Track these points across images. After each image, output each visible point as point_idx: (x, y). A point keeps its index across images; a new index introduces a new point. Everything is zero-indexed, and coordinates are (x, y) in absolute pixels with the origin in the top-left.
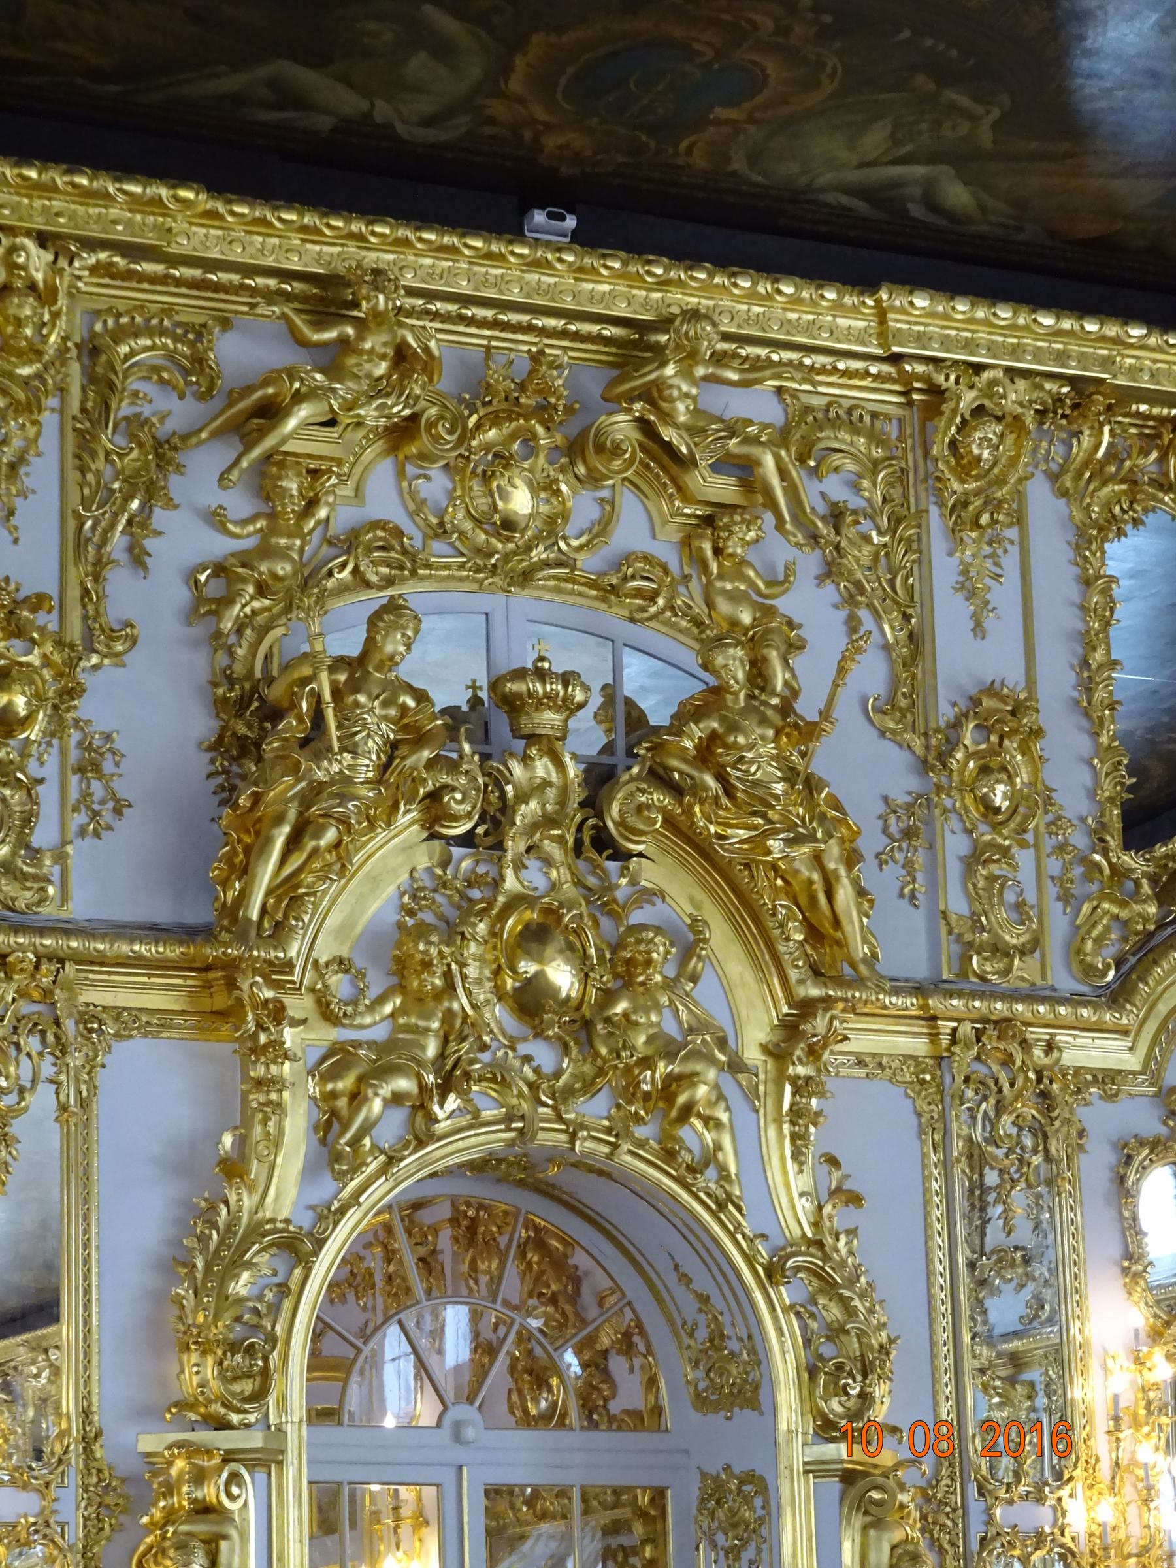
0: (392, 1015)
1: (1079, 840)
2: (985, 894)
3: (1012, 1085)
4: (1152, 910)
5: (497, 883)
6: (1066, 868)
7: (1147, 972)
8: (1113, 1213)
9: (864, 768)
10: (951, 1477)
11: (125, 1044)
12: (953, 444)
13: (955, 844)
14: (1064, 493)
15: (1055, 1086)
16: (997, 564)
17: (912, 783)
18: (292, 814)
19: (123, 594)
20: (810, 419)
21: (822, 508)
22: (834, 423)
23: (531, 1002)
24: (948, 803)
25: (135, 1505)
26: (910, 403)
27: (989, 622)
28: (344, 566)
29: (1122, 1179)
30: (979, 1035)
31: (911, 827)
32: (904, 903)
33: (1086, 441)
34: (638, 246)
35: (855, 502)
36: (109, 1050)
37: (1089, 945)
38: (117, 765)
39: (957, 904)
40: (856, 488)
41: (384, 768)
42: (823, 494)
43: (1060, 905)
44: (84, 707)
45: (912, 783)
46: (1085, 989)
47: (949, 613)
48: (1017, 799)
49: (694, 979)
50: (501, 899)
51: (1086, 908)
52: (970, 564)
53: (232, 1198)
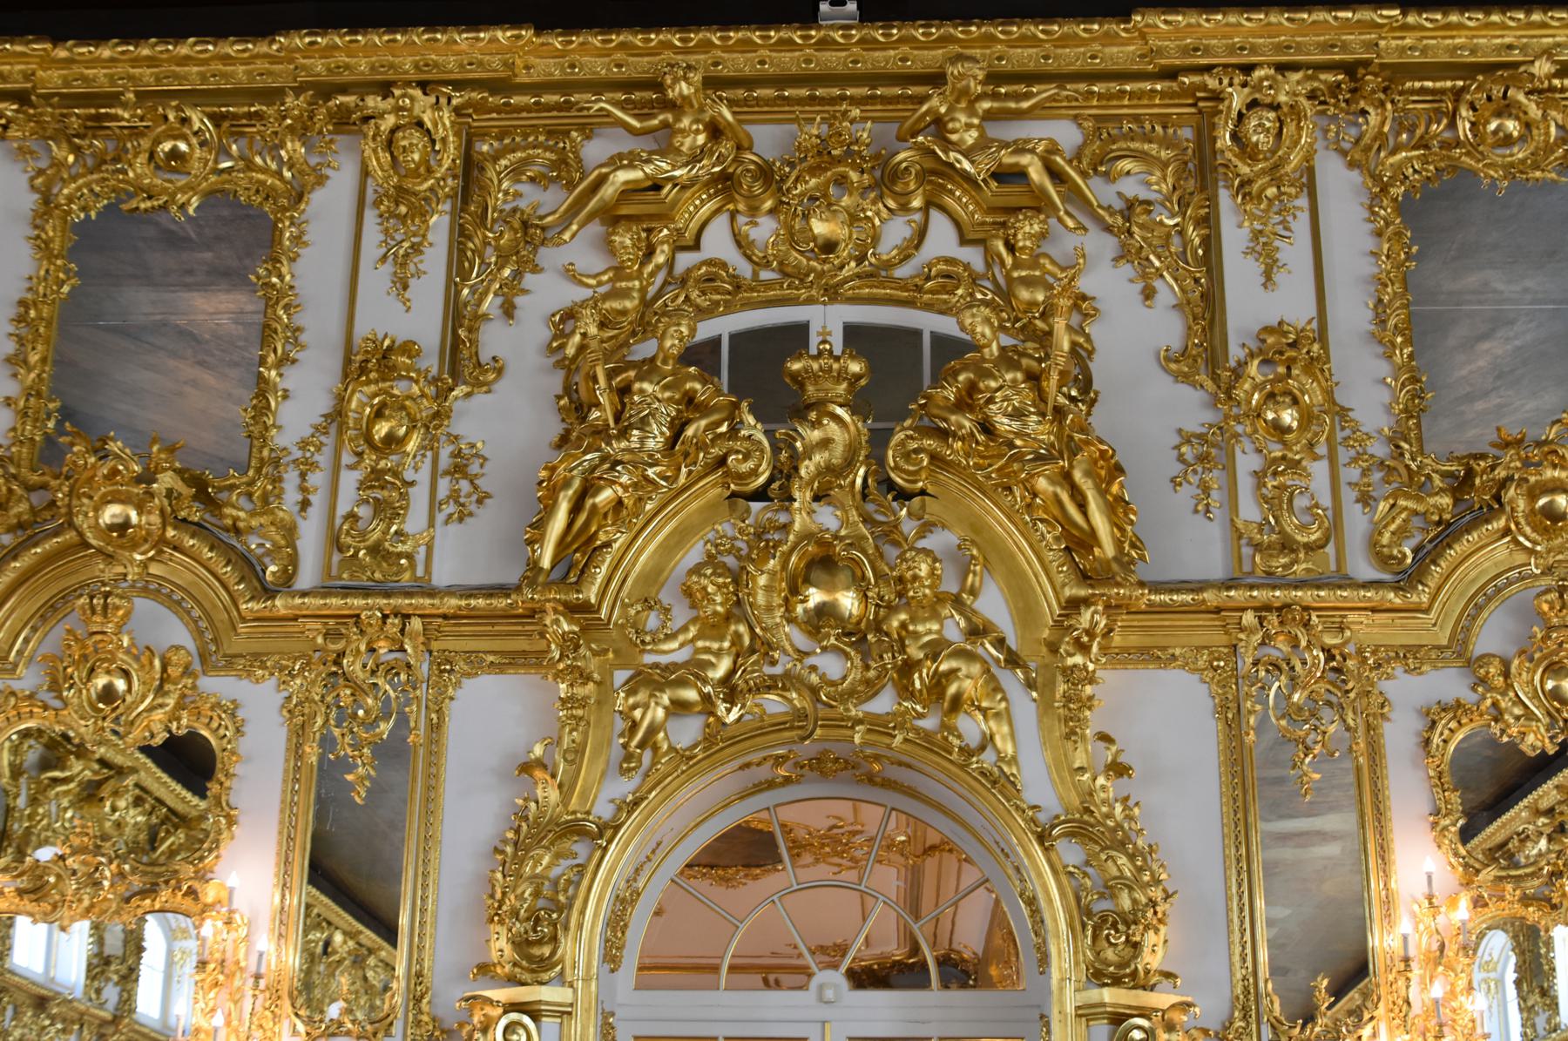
0: (692, 641)
1: (1379, 450)
2: (1277, 502)
3: (1304, 663)
4: (1446, 501)
5: (786, 528)
6: (1365, 473)
7: (1441, 555)
8: (1422, 774)
9: (1145, 403)
10: (1245, 1018)
11: (472, 681)
12: (1234, 136)
13: (1247, 462)
14: (1352, 165)
15: (1350, 663)
16: (1287, 229)
17: (1209, 416)
18: (577, 483)
19: (494, 340)
20: (1105, 135)
21: (1118, 205)
24: (1239, 429)
26: (1200, 112)
27: (1276, 277)
28: (677, 297)
29: (1427, 742)
30: (1261, 620)
31: (1206, 452)
32: (1200, 518)
33: (1374, 118)
34: (907, 14)
35: (1144, 194)
36: (458, 685)
37: (1386, 538)
38: (482, 466)
39: (1250, 511)
40: (1148, 184)
42: (1119, 194)
43: (1359, 506)
45: (1209, 416)
46: (1386, 577)
47: (1239, 271)
48: (1307, 418)
49: (973, 592)
50: (791, 537)
51: (1383, 506)
52: (1261, 232)
53: (540, 793)
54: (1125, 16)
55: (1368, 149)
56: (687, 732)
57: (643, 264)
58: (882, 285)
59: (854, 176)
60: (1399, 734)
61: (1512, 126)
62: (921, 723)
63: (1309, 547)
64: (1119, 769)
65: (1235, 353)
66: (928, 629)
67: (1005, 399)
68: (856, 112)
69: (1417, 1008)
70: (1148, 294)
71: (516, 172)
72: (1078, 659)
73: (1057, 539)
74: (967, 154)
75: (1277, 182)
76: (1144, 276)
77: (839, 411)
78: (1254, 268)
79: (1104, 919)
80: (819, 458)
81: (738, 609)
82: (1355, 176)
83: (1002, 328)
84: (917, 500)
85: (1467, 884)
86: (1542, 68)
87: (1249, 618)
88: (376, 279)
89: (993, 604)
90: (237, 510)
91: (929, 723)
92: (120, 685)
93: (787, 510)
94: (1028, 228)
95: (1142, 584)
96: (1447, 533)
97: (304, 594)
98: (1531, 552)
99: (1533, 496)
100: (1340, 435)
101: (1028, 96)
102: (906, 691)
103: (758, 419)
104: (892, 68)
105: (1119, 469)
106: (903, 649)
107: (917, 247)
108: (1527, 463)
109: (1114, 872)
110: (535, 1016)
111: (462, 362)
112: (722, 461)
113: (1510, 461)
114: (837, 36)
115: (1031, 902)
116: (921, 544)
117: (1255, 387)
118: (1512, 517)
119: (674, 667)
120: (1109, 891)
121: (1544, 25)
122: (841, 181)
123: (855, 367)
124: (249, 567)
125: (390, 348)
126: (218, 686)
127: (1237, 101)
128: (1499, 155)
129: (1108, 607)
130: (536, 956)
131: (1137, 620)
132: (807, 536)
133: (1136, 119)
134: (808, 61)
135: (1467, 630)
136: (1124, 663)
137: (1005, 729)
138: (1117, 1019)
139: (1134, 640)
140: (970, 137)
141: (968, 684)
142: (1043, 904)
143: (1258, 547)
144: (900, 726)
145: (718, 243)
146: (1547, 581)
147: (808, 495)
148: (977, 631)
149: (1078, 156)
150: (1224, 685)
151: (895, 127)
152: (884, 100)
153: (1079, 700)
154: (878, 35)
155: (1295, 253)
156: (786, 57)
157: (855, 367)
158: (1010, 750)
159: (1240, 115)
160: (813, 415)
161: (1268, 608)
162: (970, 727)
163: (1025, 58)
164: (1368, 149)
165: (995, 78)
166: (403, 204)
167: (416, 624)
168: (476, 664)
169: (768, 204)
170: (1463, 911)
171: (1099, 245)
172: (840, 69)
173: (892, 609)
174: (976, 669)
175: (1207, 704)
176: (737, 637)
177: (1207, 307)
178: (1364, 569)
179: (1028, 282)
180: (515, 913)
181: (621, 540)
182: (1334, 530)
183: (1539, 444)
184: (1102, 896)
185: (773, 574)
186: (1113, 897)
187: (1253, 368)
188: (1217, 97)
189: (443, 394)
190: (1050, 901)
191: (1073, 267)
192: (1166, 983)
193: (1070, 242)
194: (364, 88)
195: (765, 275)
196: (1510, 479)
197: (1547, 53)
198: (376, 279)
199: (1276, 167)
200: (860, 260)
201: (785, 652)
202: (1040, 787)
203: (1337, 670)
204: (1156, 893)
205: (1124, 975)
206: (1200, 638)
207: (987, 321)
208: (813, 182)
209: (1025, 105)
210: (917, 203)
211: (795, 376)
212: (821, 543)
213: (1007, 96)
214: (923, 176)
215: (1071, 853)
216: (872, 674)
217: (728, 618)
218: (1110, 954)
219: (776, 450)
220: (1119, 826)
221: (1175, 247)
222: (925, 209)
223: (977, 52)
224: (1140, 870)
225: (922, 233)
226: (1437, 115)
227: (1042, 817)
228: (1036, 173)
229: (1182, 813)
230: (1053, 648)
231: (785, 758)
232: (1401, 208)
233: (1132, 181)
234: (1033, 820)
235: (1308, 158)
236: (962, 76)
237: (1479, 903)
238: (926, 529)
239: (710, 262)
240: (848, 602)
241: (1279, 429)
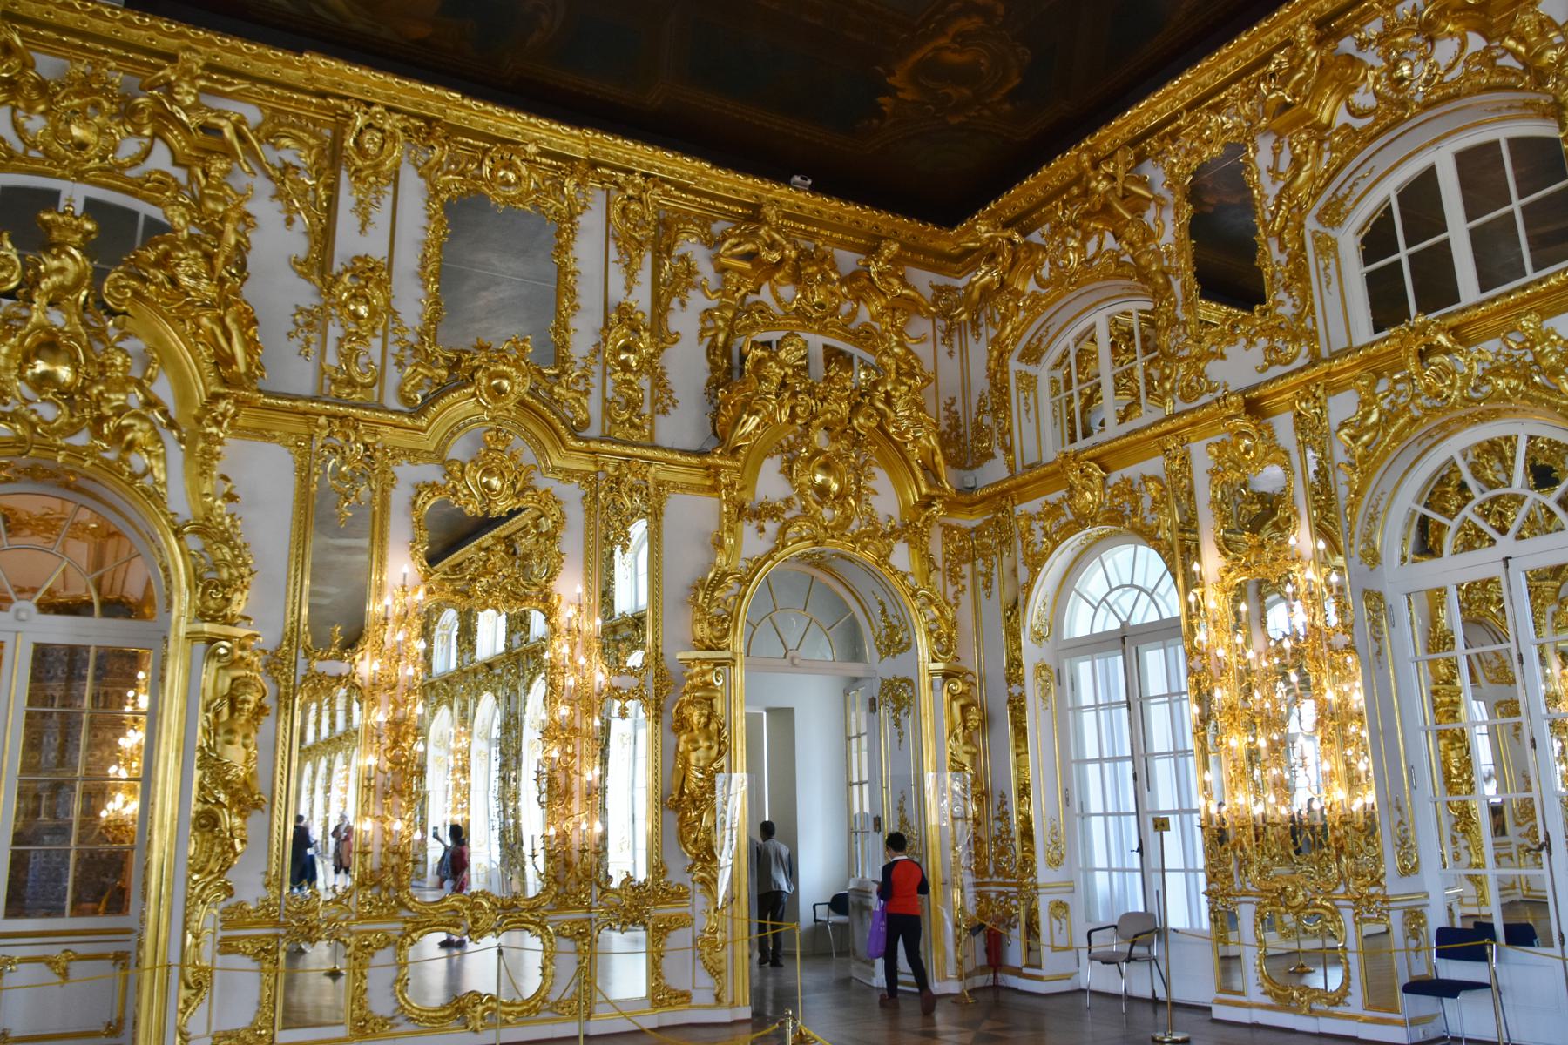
1: (412, 338)
2: (348, 357)
4: (444, 373)
5: (26, 319)
6: (402, 349)
9: (278, 288)
10: (290, 645)
12: (355, 142)
14: (421, 175)
17: (316, 301)
21: (279, 164)
22: (293, 125)
27: (369, 229)
29: (415, 502)
31: (311, 322)
33: (437, 152)
35: (295, 162)
37: (408, 388)
39: (332, 359)
45: (316, 301)
46: (405, 409)
47: (346, 220)
48: (374, 313)
49: (151, 379)
51: (409, 370)
54: (300, 53)
55: (431, 169)
58: (115, 178)
59: (106, 105)
60: (399, 497)
61: (511, 176)
62: (106, 455)
63: (364, 386)
64: (230, 497)
65: (337, 267)
66: (118, 398)
67: (187, 268)
68: (113, 64)
69: (388, 645)
70: (290, 222)
72: (214, 430)
73: (210, 356)
74: (186, 109)
75: (377, 174)
76: (289, 211)
77: (73, 251)
78: (356, 221)
79: (210, 583)
80: (55, 279)
82: (422, 182)
83: (192, 222)
84: (120, 317)
85: (425, 581)
86: (531, 149)
87: (322, 420)
89: (163, 388)
91: (111, 456)
93: (29, 308)
94: (218, 165)
95: (260, 391)
96: (442, 391)
98: (486, 408)
99: (491, 378)
100: (391, 326)
101: (231, 84)
102: (97, 433)
103: (14, 245)
104: (141, 42)
105: (255, 322)
106: (98, 407)
107: (143, 160)
108: (490, 359)
109: (220, 556)
113: (482, 357)
114: (107, 11)
115: (166, 569)
116: (120, 345)
117: (346, 289)
118: (478, 388)
120: (215, 567)
121: (536, 126)
122: (97, 106)
123: (89, 226)
128: (502, 190)
129: (237, 401)
131: (254, 412)
132: (40, 327)
133: (297, 116)
134: (83, 22)
135: (445, 444)
136: (244, 436)
137: (161, 465)
138: (211, 641)
139: (252, 423)
140: (189, 100)
141: (140, 434)
142: (172, 571)
143: (334, 381)
144: (91, 455)
146: (492, 425)
147: (45, 301)
148: (150, 403)
149: (258, 129)
150: (302, 456)
151: (138, 81)
152: (133, 61)
153: (211, 453)
154: (136, 19)
155: (381, 216)
156: (68, 15)
157: (89, 226)
158: (162, 477)
159: (361, 131)
160: (55, 251)
161: (334, 416)
162: (139, 461)
163: (233, 60)
164: (431, 169)
165: (210, 67)
169: (41, 108)
170: (420, 595)
171: (263, 186)
172: (105, 34)
173: (94, 382)
174: (146, 426)
175: (291, 466)
177: (324, 237)
178: (393, 402)
179: (214, 198)
182: (379, 378)
183: (498, 351)
184: (211, 570)
185: (12, 347)
186: (218, 571)
187: (346, 278)
188: (349, 116)
190: (177, 570)
191: (243, 196)
192: (245, 622)
193: (248, 179)
195: (32, 153)
196: (480, 367)
197: (535, 141)
199: (377, 166)
200: (103, 159)
201: (15, 398)
202: (179, 501)
203: (370, 457)
204: (245, 571)
206: (292, 427)
207: (182, 215)
208: (76, 101)
209: (228, 89)
210: (147, 132)
211: (45, 223)
212: (50, 333)
213: (217, 81)
214: (154, 117)
215: (195, 543)
216: (75, 420)
218: (211, 604)
219: (25, 267)
220: (227, 530)
221: (310, 197)
222: (153, 137)
223: (201, 48)
224: (236, 557)
225: (147, 153)
226: (472, 160)
227: (179, 520)
228: (228, 132)
229: (268, 526)
230: (199, 420)
231: (7, 466)
232: (446, 206)
233: (289, 151)
234: (172, 522)
235: (397, 165)
236: (188, 60)
237: (430, 591)
238: (124, 336)
240: (64, 373)
241: (356, 316)
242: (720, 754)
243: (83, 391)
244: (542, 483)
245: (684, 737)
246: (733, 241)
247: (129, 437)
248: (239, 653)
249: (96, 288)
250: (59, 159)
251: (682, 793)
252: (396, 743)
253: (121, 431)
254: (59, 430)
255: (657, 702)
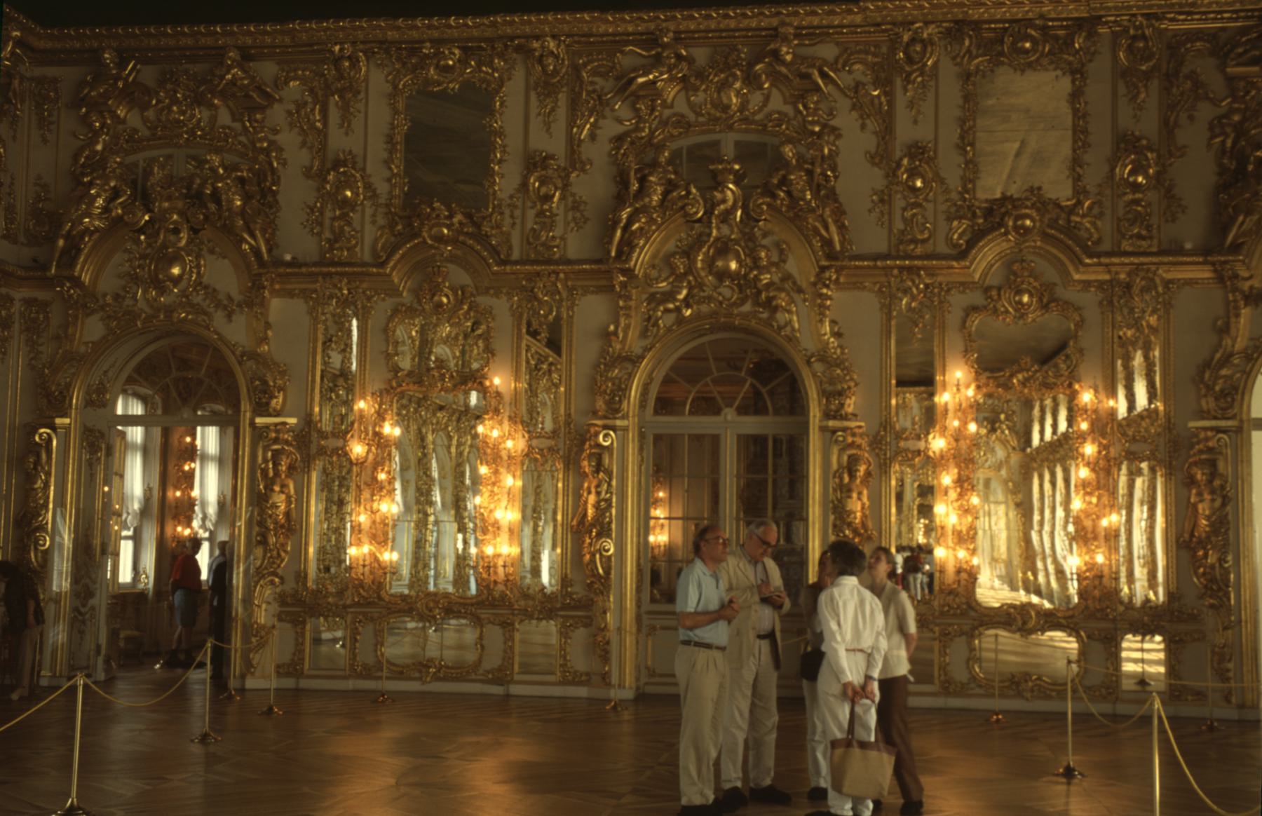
1: (954, 196)
5: (710, 235)
9: (857, 180)
17: (885, 182)
19: (587, 151)
21: (853, 84)
22: (859, 52)
23: (723, 275)
25: (583, 443)
31: (884, 199)
35: (864, 79)
39: (899, 225)
41: (663, 202)
44: (574, 189)
49: (784, 261)
56: (671, 318)
57: (650, 115)
63: (924, 241)
65: (898, 154)
71: (595, 73)
76: (861, 117)
81: (690, 270)
85: (976, 379)
87: (896, 272)
88: (536, 124)
89: (791, 266)
90: (486, 228)
92: (445, 300)
97: (516, 263)
99: (1016, 220)
102: (757, 303)
110: (615, 431)
111: (575, 160)
112: (683, 208)
119: (663, 294)
122: (734, 75)
123: (737, 167)
124: (495, 251)
125: (545, 158)
126: (483, 301)
127: (906, 38)
130: (614, 409)
137: (795, 318)
138: (834, 432)
145: (681, 107)
157: (737, 167)
166: (545, 87)
167: (562, 275)
168: (586, 292)
170: (971, 392)
171: (843, 103)
173: (751, 270)
176: (689, 282)
177: (887, 131)
180: (605, 392)
181: (642, 242)
187: (905, 161)
189: (568, 176)
194: (527, 37)
195: (701, 119)
198: (536, 124)
202: (808, 344)
204: (852, 384)
205: (837, 414)
215: (819, 367)
217: (686, 274)
218: (833, 407)
225: (767, 98)
237: (978, 387)
238: (765, 235)
239: (675, 115)
241: (914, 189)
242: (1224, 505)
243: (746, 275)
244: (1070, 294)
245: (1194, 491)
246: (1240, 50)
247: (774, 303)
248: (850, 440)
249: (745, 208)
250: (717, 119)
251: (1192, 535)
252: (961, 496)
253: (770, 299)
254: (735, 304)
255: (1170, 463)
